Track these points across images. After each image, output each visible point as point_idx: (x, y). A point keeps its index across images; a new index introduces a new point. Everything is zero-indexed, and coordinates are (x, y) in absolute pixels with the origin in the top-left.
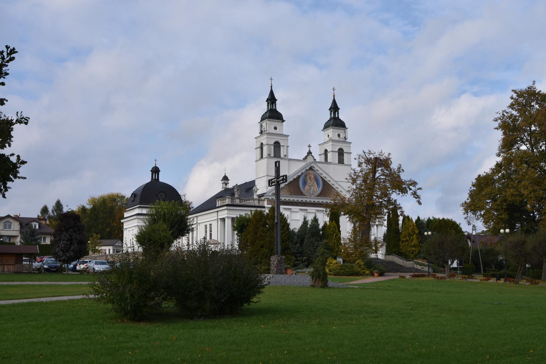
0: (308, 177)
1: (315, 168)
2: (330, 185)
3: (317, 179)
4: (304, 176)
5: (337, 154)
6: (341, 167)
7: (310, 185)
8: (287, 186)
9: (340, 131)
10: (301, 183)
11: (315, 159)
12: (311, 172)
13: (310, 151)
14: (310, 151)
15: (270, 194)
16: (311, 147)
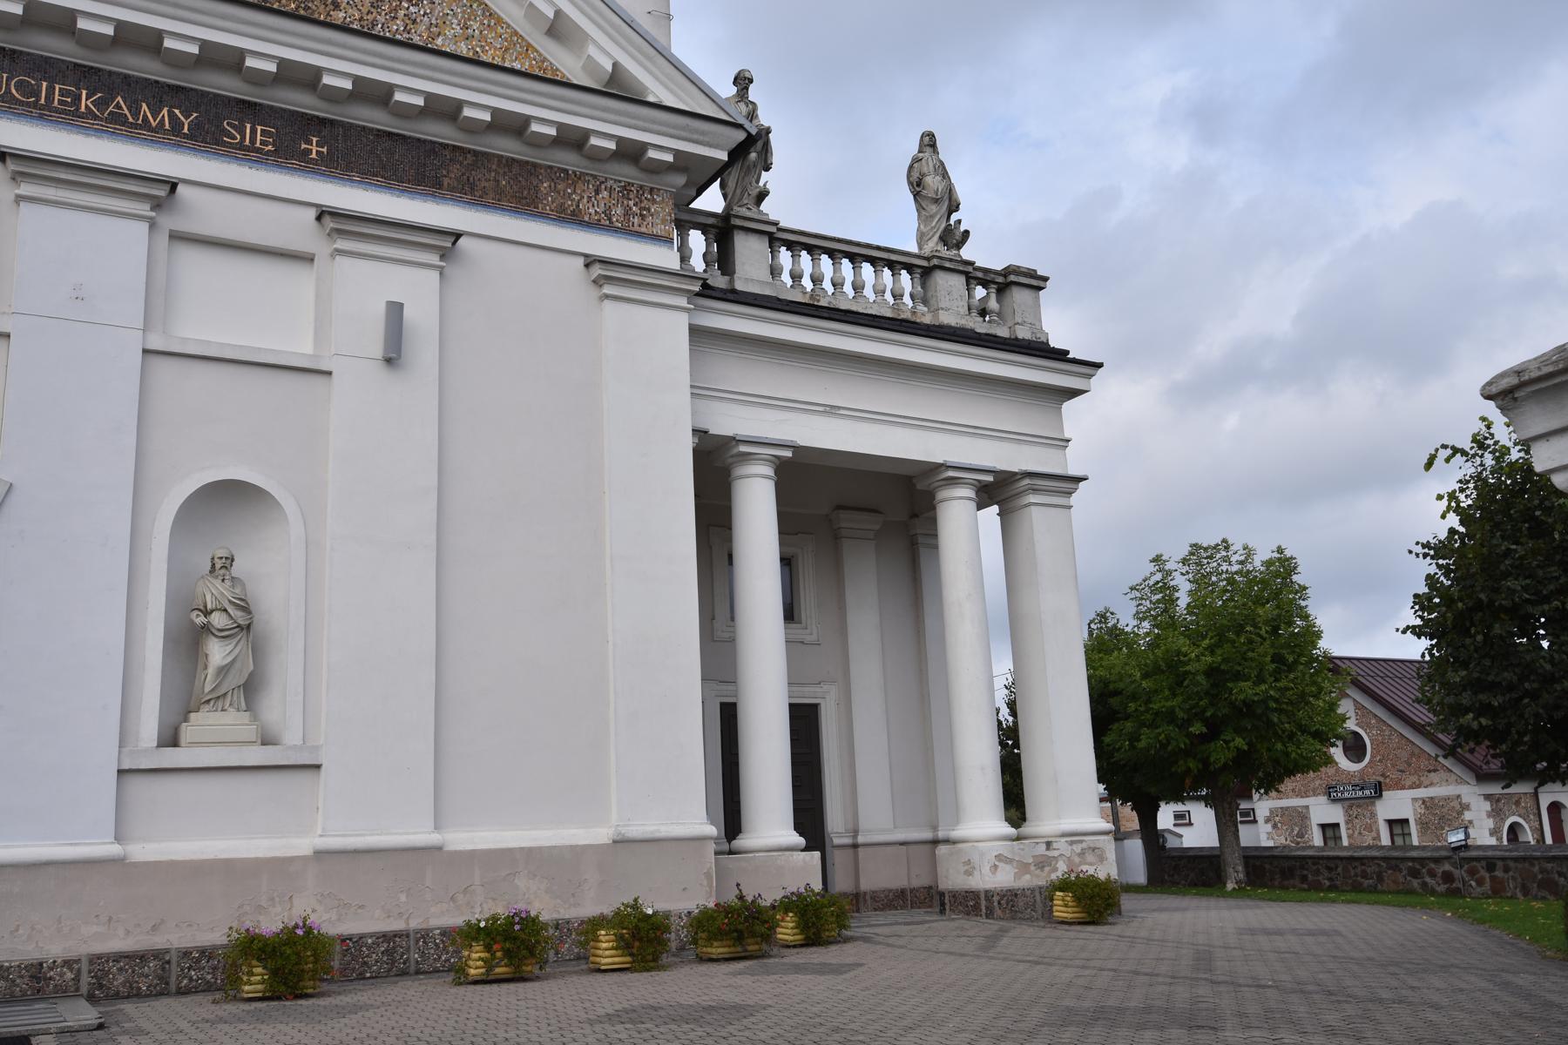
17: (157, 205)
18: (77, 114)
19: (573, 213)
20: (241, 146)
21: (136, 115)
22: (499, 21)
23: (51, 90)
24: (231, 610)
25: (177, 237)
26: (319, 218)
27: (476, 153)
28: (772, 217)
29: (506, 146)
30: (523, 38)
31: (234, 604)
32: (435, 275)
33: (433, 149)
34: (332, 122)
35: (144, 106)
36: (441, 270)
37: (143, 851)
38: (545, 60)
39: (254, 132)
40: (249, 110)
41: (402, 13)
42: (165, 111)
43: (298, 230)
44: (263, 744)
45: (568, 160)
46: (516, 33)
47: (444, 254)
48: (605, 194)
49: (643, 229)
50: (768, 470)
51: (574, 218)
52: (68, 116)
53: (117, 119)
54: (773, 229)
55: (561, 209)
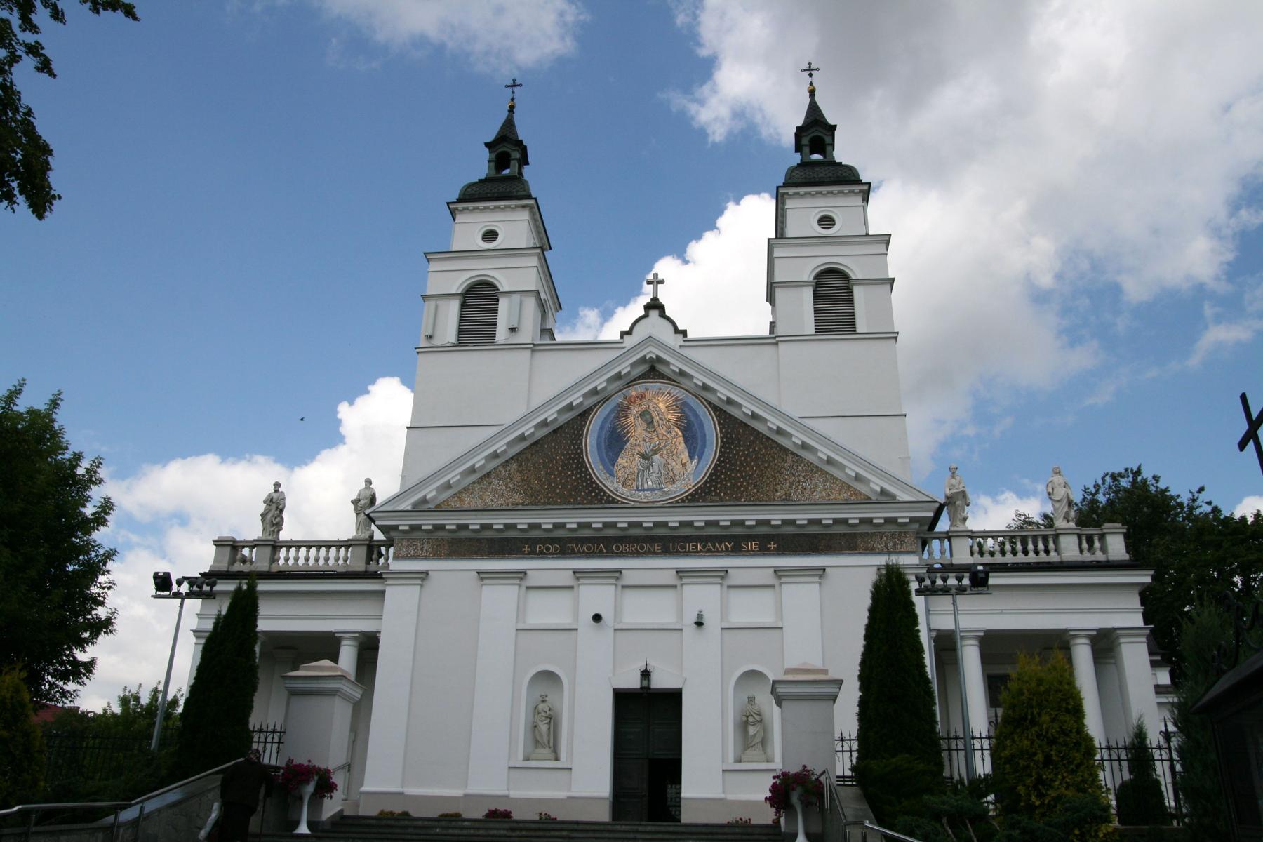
0: (636, 410)
1: (667, 363)
2: (768, 438)
3: (686, 417)
4: (609, 409)
5: (807, 294)
6: (836, 350)
7: (645, 448)
8: (514, 466)
9: (839, 204)
10: (595, 442)
11: (680, 327)
12: (654, 386)
13: (655, 299)
14: (655, 299)
15: (407, 505)
16: (662, 282)
17: (722, 578)
18: (698, 552)
19: (872, 549)
20: (748, 551)
21: (714, 547)
22: (837, 479)
23: (689, 546)
24: (754, 715)
25: (729, 587)
26: (775, 571)
27: (831, 534)
28: (970, 528)
29: (840, 529)
30: (846, 483)
31: (755, 713)
32: (817, 585)
33: (815, 536)
34: (778, 534)
35: (717, 544)
36: (820, 583)
37: (730, 797)
38: (856, 490)
39: (751, 545)
40: (750, 538)
41: (800, 487)
42: (723, 544)
43: (768, 578)
44: (768, 761)
45: (865, 529)
46: (844, 483)
47: (820, 576)
48: (885, 538)
49: (902, 550)
50: (975, 642)
51: (870, 551)
52: (695, 553)
53: (709, 550)
54: (970, 534)
55: (867, 549)
